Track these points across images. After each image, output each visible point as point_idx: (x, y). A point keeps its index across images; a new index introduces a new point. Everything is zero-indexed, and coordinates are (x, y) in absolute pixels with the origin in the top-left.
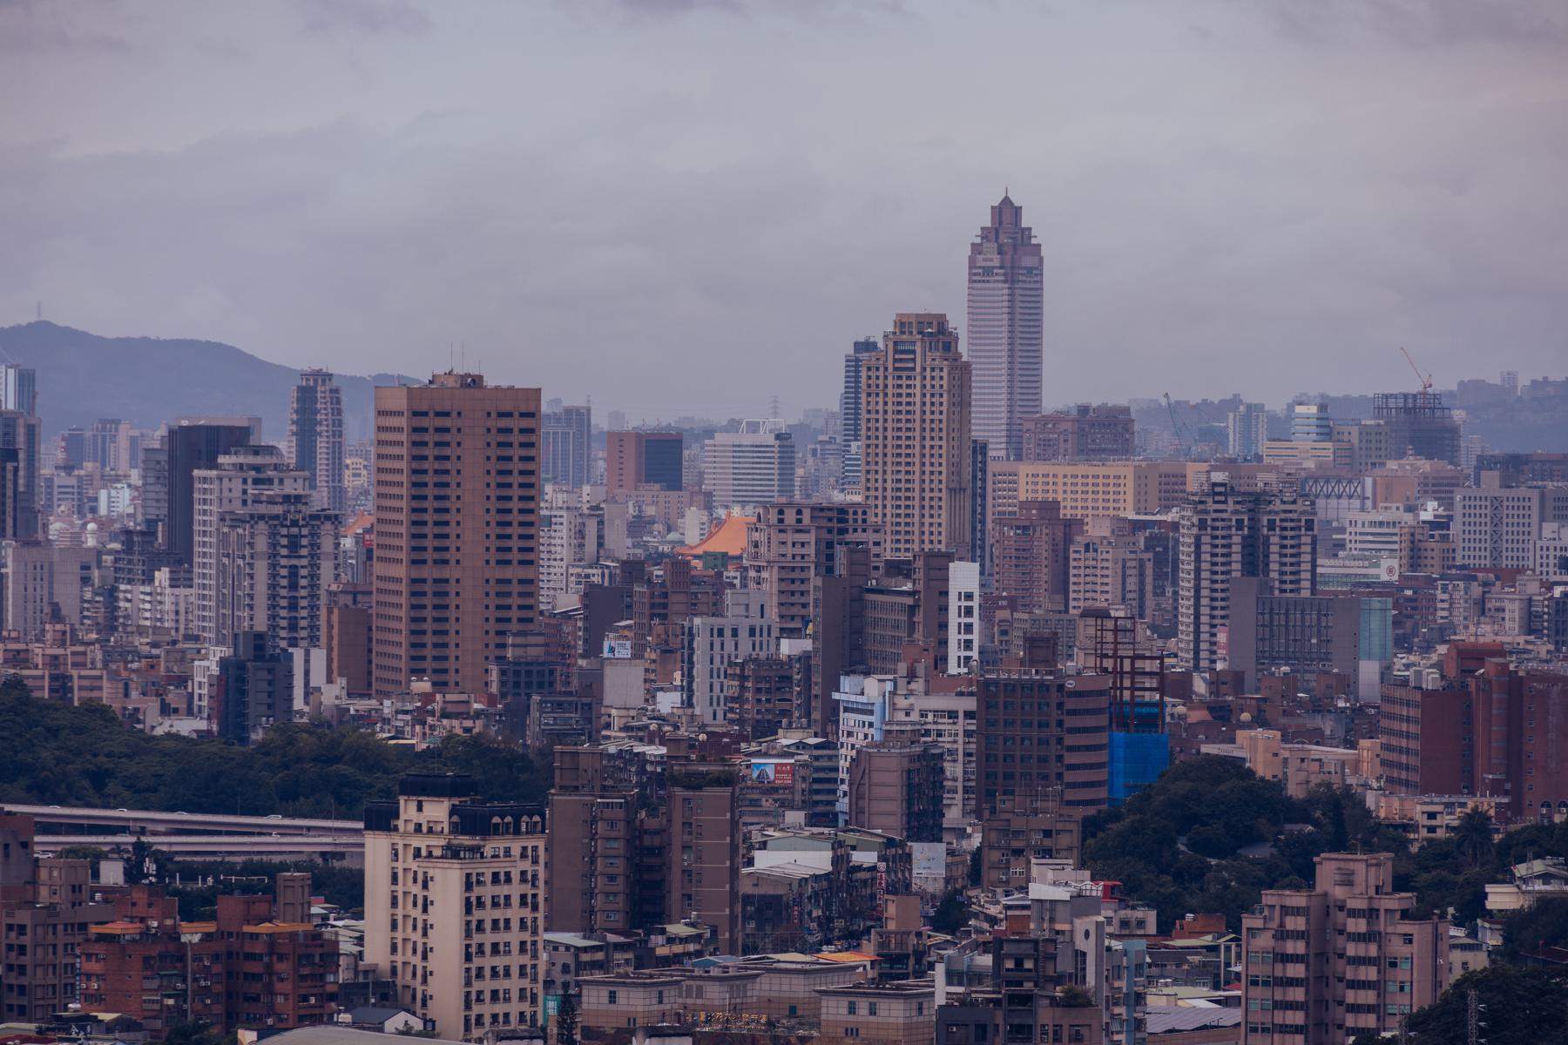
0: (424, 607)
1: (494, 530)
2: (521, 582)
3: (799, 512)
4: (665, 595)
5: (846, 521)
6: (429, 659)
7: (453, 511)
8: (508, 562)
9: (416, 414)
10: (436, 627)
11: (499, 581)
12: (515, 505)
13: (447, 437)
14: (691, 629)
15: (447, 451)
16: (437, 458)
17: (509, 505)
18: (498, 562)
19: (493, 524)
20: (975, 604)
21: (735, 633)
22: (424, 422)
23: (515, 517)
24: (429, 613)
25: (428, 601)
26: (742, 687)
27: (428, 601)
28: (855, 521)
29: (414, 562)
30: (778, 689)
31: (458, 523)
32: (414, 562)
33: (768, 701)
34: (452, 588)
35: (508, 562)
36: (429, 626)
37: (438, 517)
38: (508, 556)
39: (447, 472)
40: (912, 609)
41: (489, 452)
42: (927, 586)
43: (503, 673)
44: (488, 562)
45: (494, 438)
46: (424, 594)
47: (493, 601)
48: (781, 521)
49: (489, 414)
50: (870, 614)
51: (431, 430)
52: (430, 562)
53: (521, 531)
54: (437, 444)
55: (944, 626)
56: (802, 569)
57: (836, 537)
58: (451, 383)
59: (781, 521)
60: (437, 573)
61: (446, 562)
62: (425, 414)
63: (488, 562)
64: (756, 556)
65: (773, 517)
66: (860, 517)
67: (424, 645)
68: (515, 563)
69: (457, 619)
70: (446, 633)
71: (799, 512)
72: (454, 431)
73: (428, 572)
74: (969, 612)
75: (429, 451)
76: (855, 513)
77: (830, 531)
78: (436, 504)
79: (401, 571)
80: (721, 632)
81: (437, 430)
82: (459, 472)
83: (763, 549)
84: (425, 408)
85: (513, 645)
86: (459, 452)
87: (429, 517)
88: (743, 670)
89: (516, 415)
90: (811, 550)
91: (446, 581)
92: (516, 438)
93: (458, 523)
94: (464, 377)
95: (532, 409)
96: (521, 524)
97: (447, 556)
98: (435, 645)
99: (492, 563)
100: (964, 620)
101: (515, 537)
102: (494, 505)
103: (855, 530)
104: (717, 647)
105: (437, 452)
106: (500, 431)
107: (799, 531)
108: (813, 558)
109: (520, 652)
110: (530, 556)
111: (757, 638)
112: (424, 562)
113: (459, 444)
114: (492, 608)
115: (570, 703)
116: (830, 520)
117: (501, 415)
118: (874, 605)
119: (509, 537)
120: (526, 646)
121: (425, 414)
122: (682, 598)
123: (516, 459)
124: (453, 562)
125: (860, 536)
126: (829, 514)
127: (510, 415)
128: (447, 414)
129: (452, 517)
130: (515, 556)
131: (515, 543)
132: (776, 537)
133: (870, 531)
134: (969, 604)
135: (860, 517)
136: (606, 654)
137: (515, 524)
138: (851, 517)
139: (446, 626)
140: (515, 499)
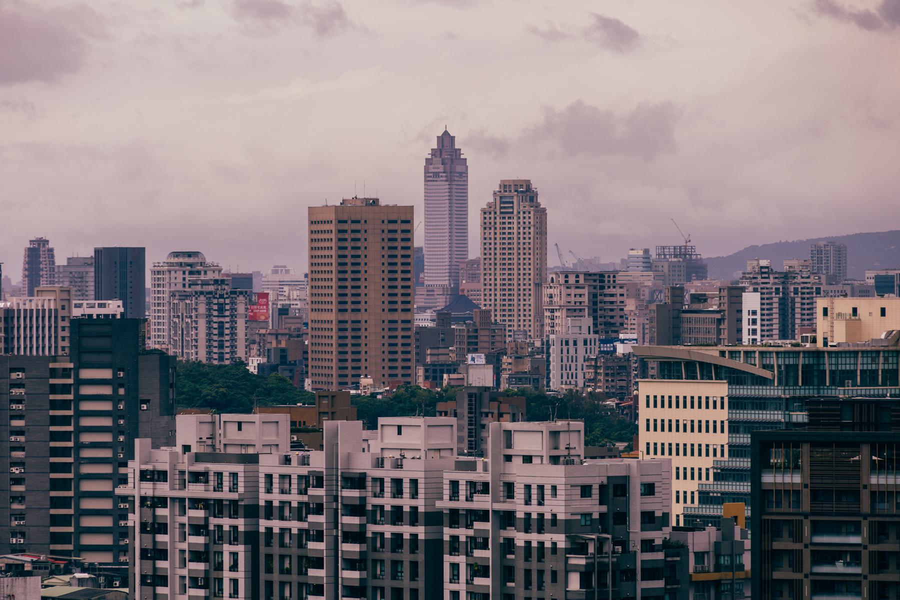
0: (346, 337)
1: (387, 291)
2: (403, 322)
3: (577, 276)
4: (476, 331)
5: (604, 281)
6: (350, 368)
7: (363, 279)
8: (396, 310)
9: (340, 222)
10: (353, 349)
11: (390, 322)
12: (399, 276)
13: (358, 236)
14: (548, 341)
15: (359, 244)
16: (353, 248)
17: (396, 276)
18: (390, 310)
19: (386, 287)
20: (758, 317)
21: (575, 343)
22: (345, 227)
23: (399, 283)
24: (349, 341)
25: (349, 334)
26: (596, 373)
27: (349, 334)
28: (609, 281)
29: (340, 310)
30: (618, 374)
31: (366, 287)
32: (340, 310)
33: (612, 381)
34: (363, 326)
35: (396, 310)
36: (349, 349)
37: (354, 284)
38: (396, 307)
39: (359, 256)
40: (719, 321)
41: (384, 244)
42: (729, 307)
43: (426, 371)
44: (383, 310)
45: (387, 236)
46: (346, 330)
47: (387, 333)
48: (566, 282)
49: (383, 222)
50: (686, 326)
51: (349, 231)
52: (349, 311)
53: (403, 291)
54: (353, 240)
55: (740, 330)
56: (580, 310)
57: (599, 291)
58: (358, 203)
59: (566, 282)
60: (354, 316)
61: (359, 310)
62: (346, 222)
63: (383, 310)
64: (551, 303)
65: (562, 279)
66: (612, 279)
67: (346, 360)
68: (400, 310)
69: (366, 345)
70: (359, 353)
71: (577, 276)
72: (363, 232)
73: (348, 316)
74: (754, 322)
75: (348, 244)
76: (609, 277)
77: (595, 288)
78: (353, 276)
79: (332, 316)
80: (567, 343)
81: (353, 231)
82: (366, 256)
83: (555, 299)
84: (345, 218)
85: (431, 354)
86: (366, 244)
87: (349, 284)
88: (596, 363)
89: (399, 222)
90: (585, 299)
91: (359, 322)
92: (399, 236)
93: (366, 287)
94: (367, 200)
95: (408, 218)
96: (403, 287)
97: (359, 306)
98: (353, 360)
99: (386, 310)
100: (751, 327)
101: (399, 295)
102: (386, 276)
103: (609, 287)
104: (565, 352)
105: (353, 244)
106: (390, 231)
107: (577, 288)
108: (586, 303)
109: (435, 358)
110: (408, 306)
111: (588, 346)
112: (346, 310)
113: (366, 239)
114: (386, 338)
115: (526, 379)
116: (595, 281)
117: (390, 222)
118: (690, 321)
119: (396, 295)
120: (438, 355)
121: (346, 222)
122: (486, 333)
123: (399, 248)
124: (363, 311)
125: (612, 291)
126: (595, 278)
127: (396, 222)
128: (358, 222)
129: (362, 283)
130: (400, 306)
131: (399, 299)
132: (564, 291)
133: (618, 288)
134: (754, 317)
135: (612, 279)
136: (470, 362)
137: (399, 287)
138: (606, 279)
139: (359, 349)
140: (399, 272)
